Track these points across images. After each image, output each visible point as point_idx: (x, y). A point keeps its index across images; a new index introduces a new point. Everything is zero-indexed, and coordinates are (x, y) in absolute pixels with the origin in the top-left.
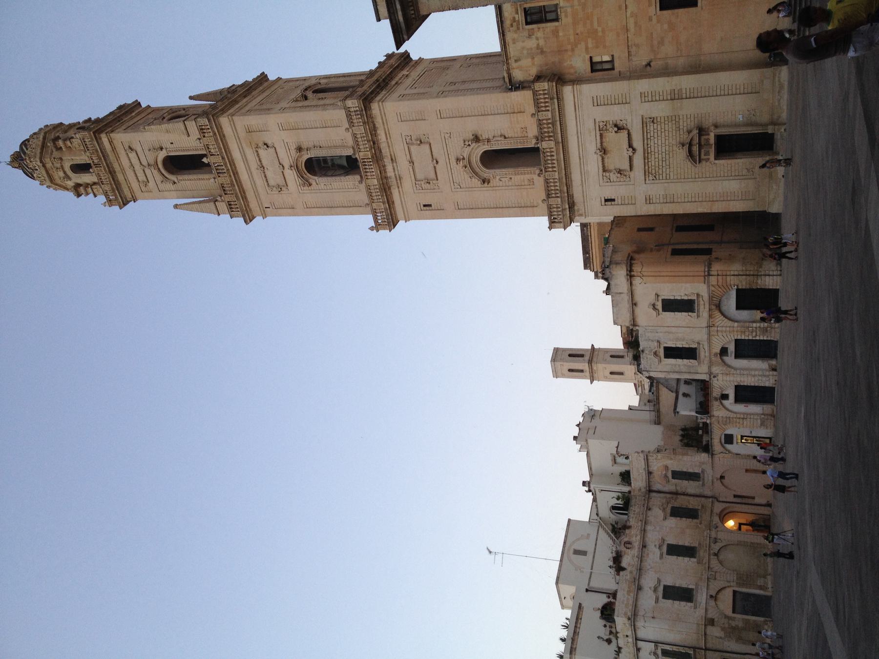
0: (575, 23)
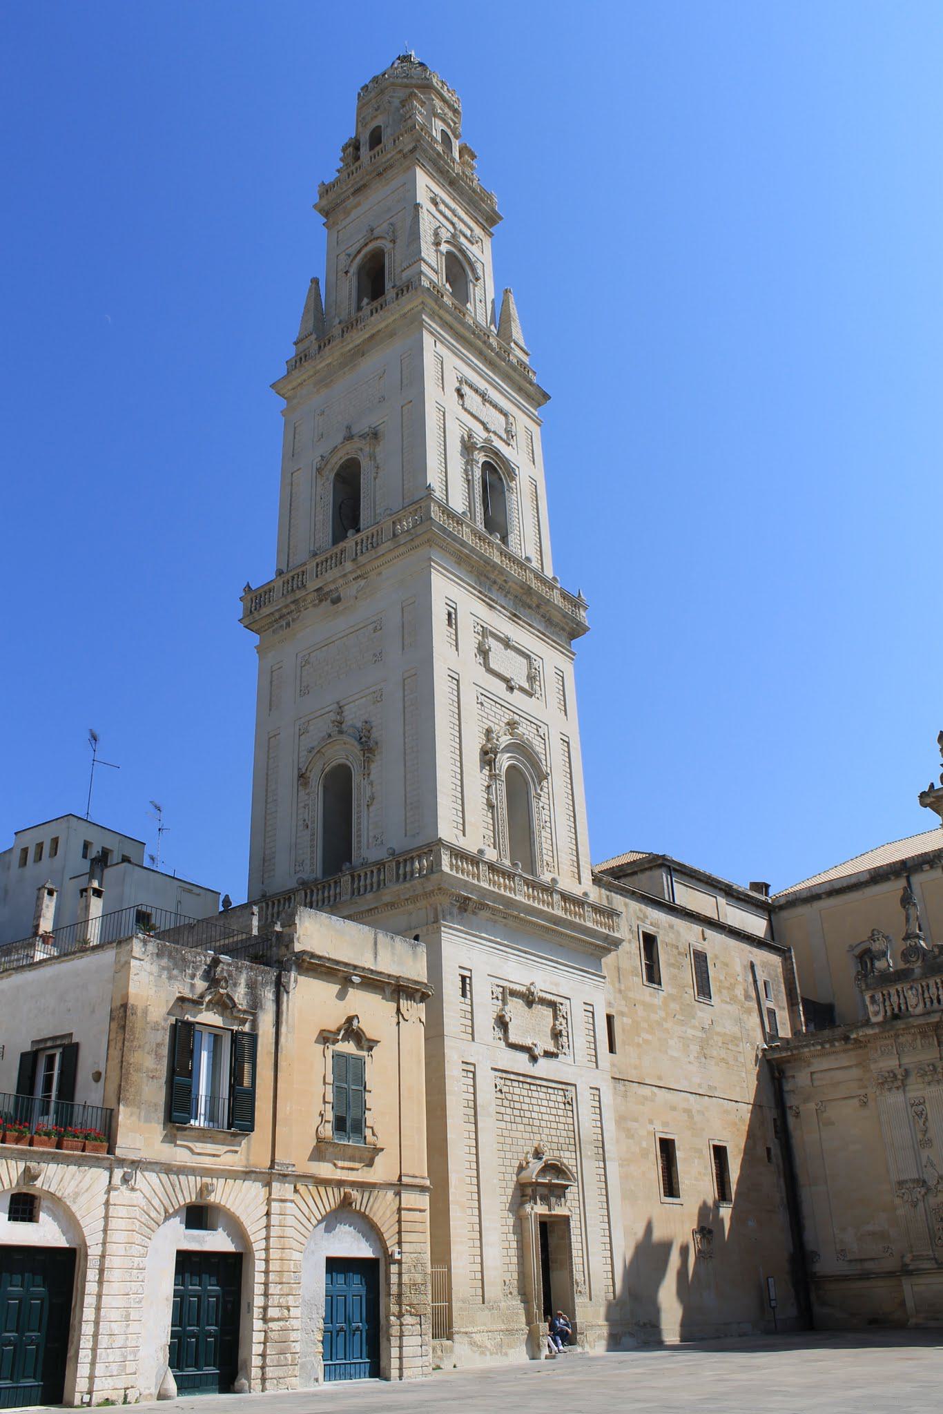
0: (644, 1004)
